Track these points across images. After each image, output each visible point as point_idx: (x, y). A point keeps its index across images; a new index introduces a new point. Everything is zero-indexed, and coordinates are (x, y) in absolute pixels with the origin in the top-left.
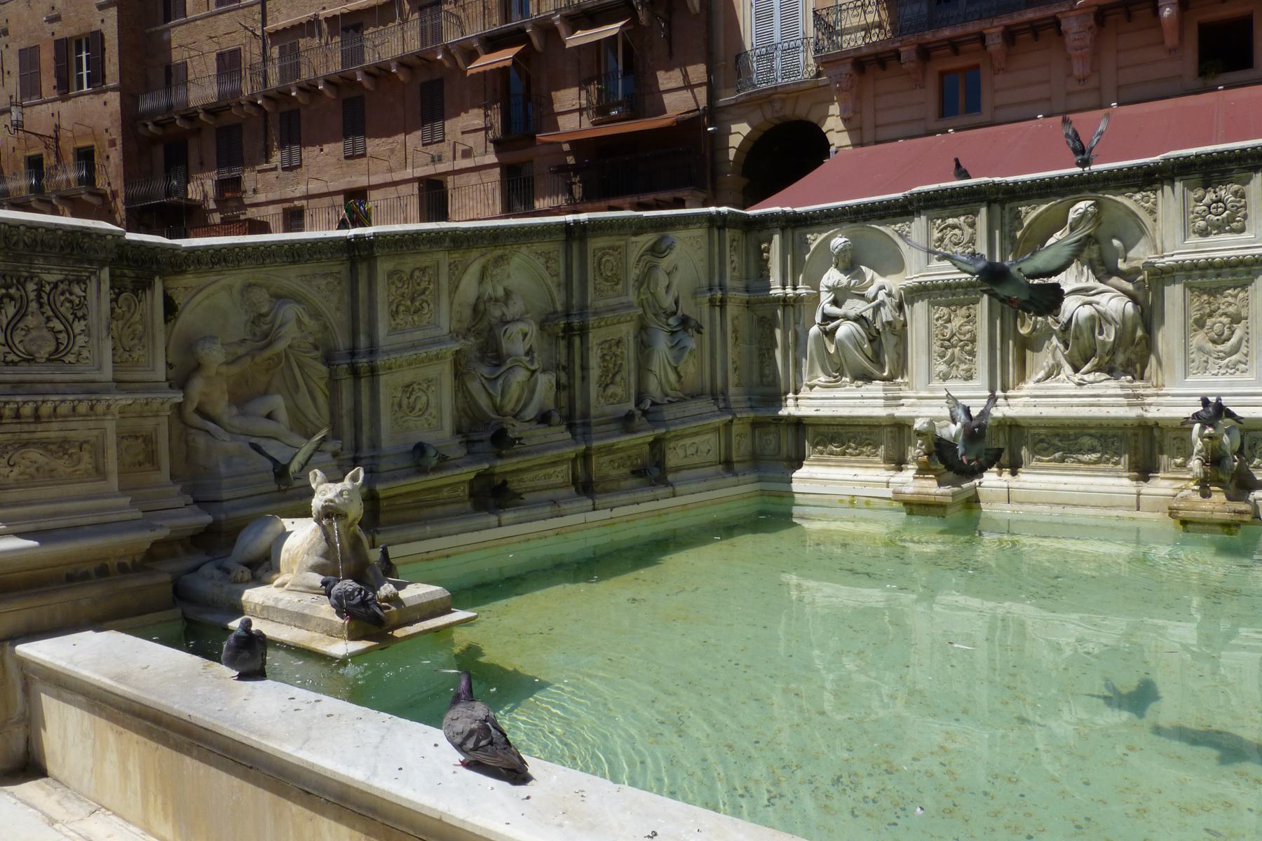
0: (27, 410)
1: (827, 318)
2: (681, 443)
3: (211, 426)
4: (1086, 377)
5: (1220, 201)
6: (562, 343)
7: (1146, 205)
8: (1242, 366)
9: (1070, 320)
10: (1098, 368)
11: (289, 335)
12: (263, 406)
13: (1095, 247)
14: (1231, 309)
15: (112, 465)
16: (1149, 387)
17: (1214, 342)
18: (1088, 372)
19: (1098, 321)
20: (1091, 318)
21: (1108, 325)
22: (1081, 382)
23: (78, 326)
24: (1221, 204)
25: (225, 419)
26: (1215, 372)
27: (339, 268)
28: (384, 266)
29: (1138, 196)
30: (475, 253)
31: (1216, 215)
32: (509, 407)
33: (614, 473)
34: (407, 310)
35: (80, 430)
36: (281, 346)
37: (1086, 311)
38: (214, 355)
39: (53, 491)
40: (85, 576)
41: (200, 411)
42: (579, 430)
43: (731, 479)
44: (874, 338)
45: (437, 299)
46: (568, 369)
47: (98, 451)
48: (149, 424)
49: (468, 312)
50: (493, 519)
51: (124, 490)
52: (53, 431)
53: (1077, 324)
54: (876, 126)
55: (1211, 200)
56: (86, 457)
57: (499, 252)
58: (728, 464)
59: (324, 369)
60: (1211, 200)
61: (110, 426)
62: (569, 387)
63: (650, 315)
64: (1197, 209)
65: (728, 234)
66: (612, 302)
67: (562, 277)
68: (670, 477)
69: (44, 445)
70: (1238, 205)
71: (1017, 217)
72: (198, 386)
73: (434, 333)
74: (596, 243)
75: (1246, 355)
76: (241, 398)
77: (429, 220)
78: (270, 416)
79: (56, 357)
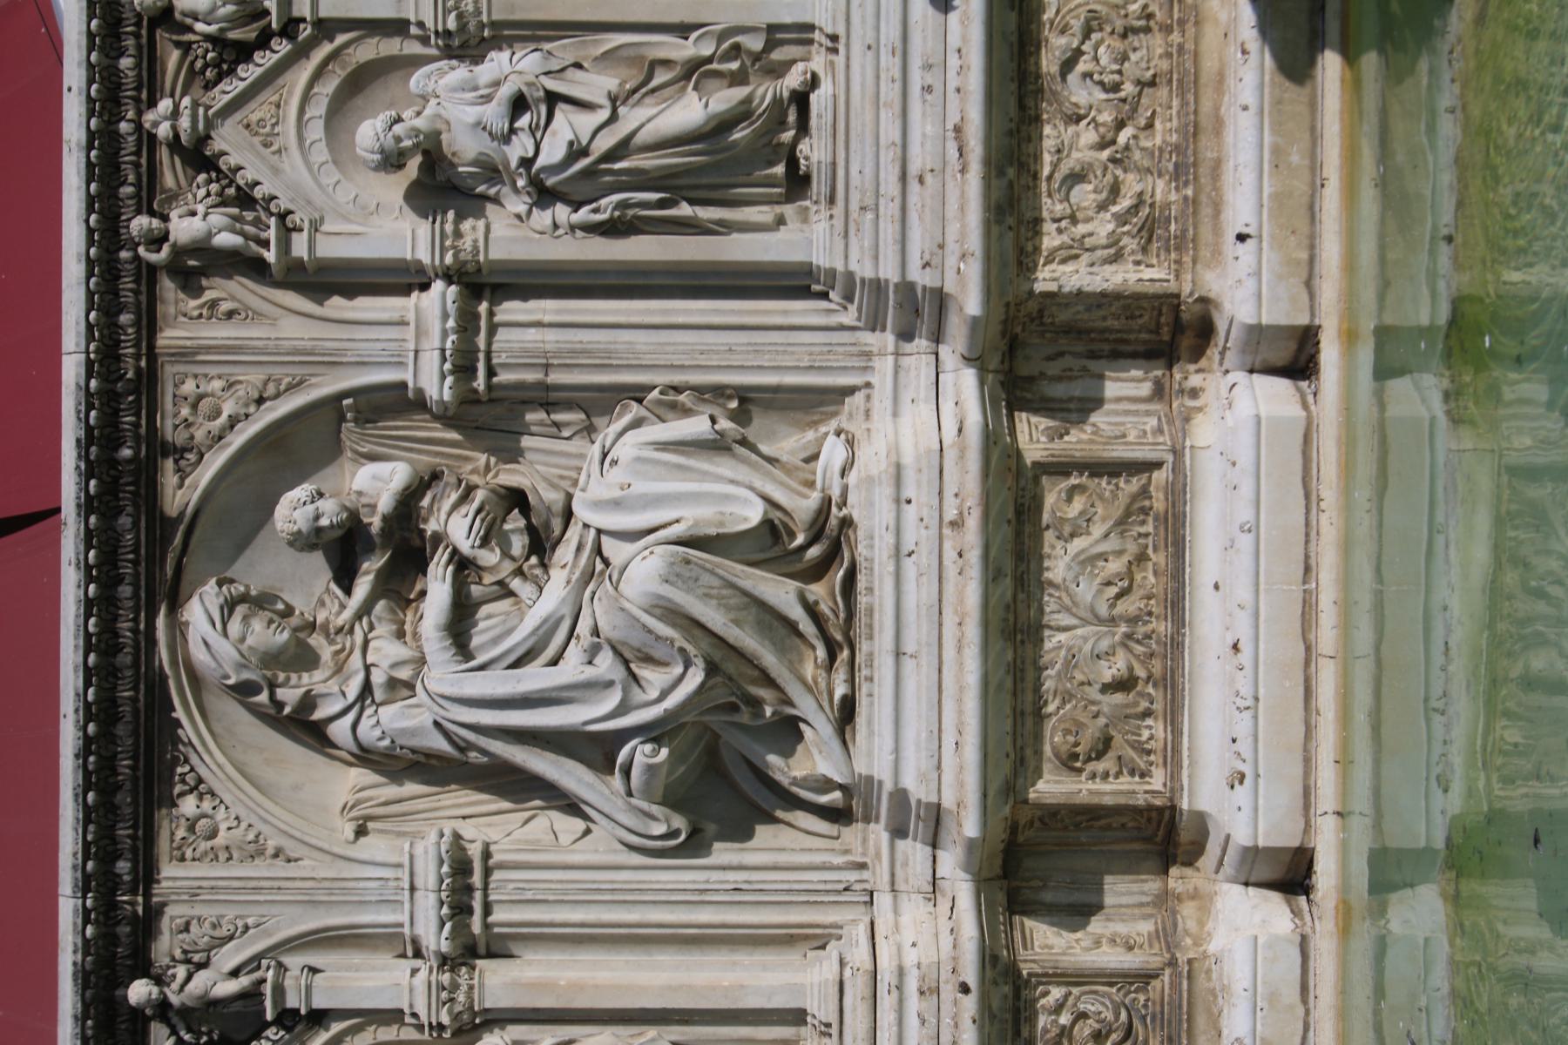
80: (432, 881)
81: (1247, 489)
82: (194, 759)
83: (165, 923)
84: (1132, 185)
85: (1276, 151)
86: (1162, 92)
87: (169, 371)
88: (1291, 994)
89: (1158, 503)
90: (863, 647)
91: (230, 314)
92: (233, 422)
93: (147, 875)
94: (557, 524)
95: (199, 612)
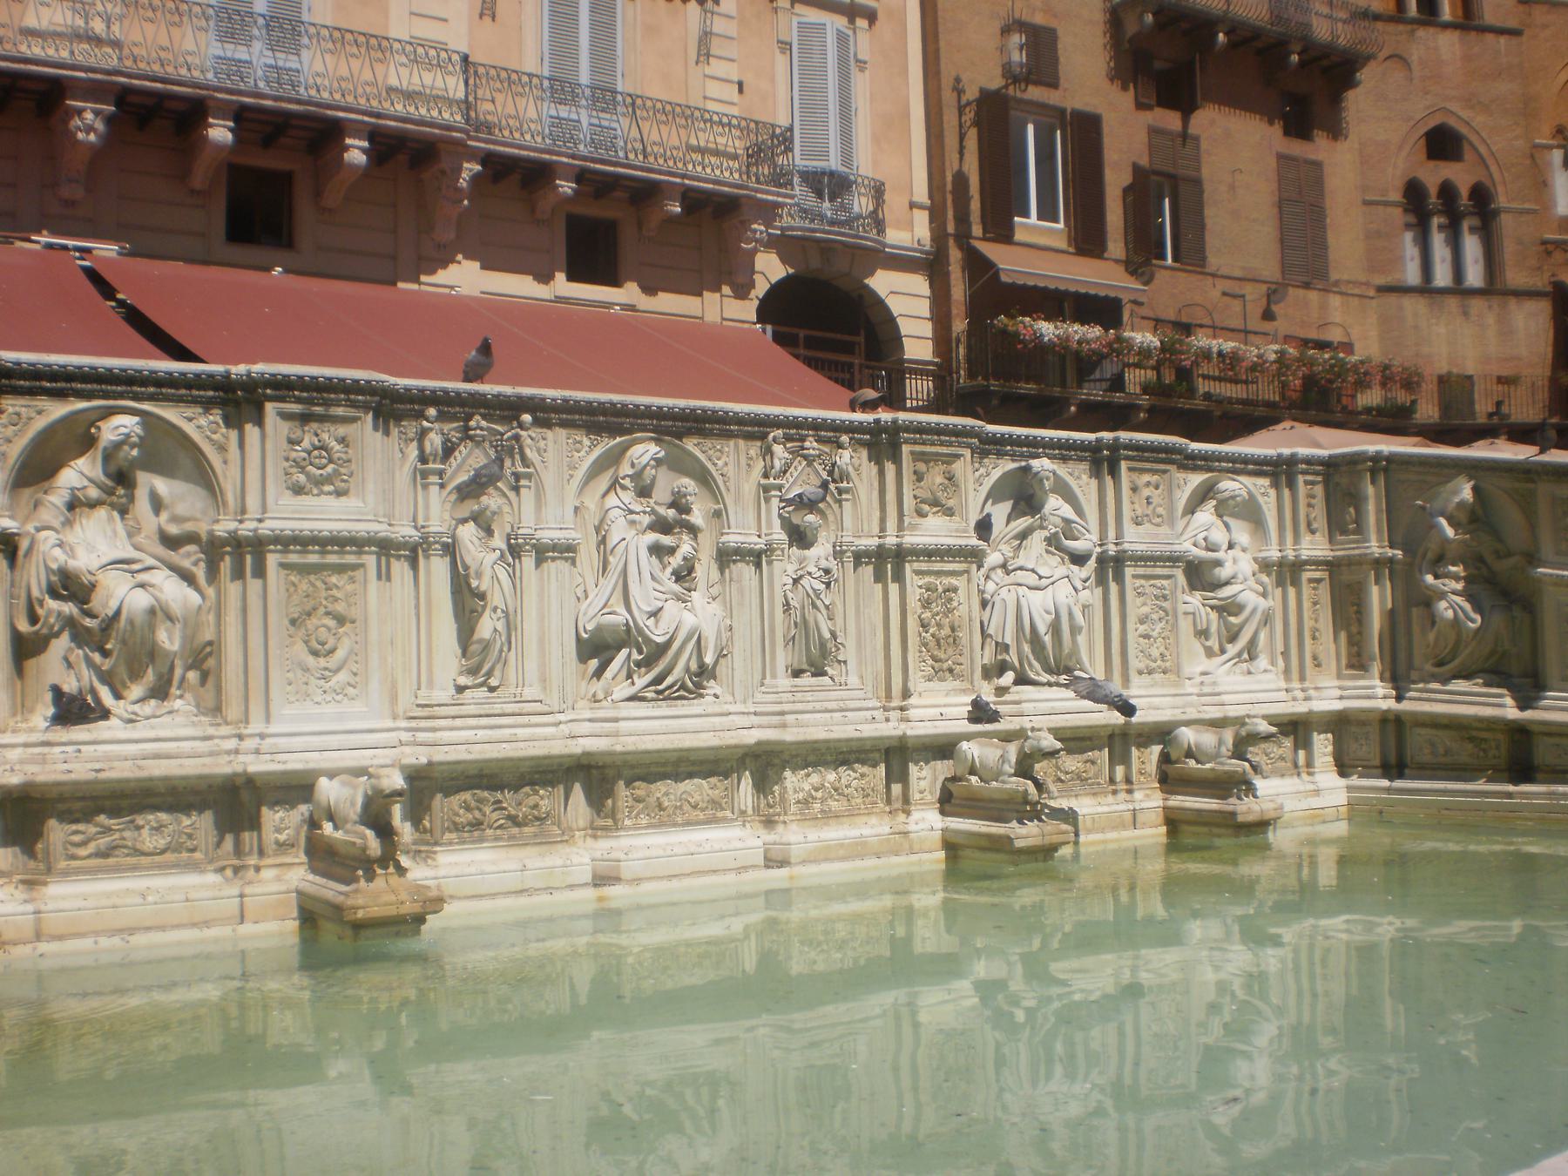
4: (136, 708)
5: (321, 448)
7: (214, 437)
8: (350, 691)
9: (118, 613)
14: (340, 608)
16: (219, 725)
17: (315, 653)
18: (141, 700)
19: (158, 613)
20: (152, 612)
21: (169, 624)
22: (134, 717)
24: (324, 453)
26: (319, 699)
29: (203, 421)
31: (319, 468)
53: (131, 622)
55: (313, 445)
60: (313, 445)
64: (294, 455)
70: (343, 456)
75: (355, 674)
80: (568, 536)
81: (731, 846)
82: (603, 444)
83: (545, 430)
84: (819, 794)
85: (842, 845)
86: (845, 803)
87: (732, 443)
88: (571, 881)
89: (720, 814)
90: (663, 703)
91: (749, 465)
92: (715, 465)
93: (564, 424)
94: (687, 585)
95: (653, 449)
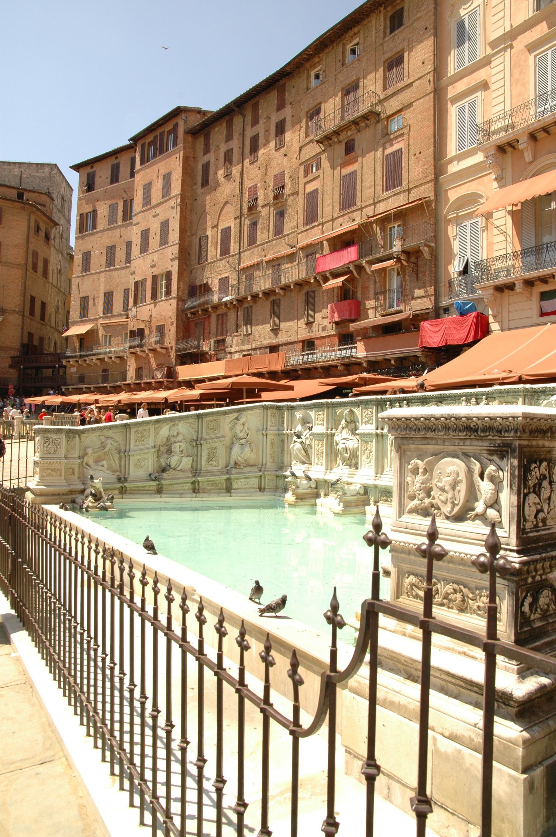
0: (49, 462)
1: (295, 442)
2: (242, 480)
3: (88, 467)
6: (195, 448)
10: (347, 465)
11: (108, 447)
12: (101, 463)
13: (353, 424)
15: (63, 474)
20: (342, 448)
23: (59, 447)
25: (92, 466)
27: (123, 430)
28: (133, 430)
30: (165, 424)
32: (172, 466)
33: (209, 488)
34: (140, 440)
35: (56, 467)
36: (107, 449)
37: (344, 446)
38: (90, 451)
39: (52, 478)
40: (56, 495)
41: (87, 464)
42: (197, 474)
43: (261, 493)
44: (306, 451)
45: (149, 438)
46: (197, 456)
47: (61, 471)
48: (74, 466)
49: (165, 440)
50: (159, 496)
51: (65, 479)
52: (53, 467)
54: (509, 321)
56: (58, 472)
57: (174, 423)
58: (261, 489)
59: (118, 455)
61: (63, 467)
62: (197, 461)
63: (234, 439)
65: (269, 411)
66: (212, 436)
67: (196, 429)
68: (233, 491)
69: (51, 469)
71: (336, 413)
72: (86, 458)
73: (147, 446)
74: (206, 419)
76: (97, 462)
77: (154, 415)
78: (103, 466)
79: (54, 453)
